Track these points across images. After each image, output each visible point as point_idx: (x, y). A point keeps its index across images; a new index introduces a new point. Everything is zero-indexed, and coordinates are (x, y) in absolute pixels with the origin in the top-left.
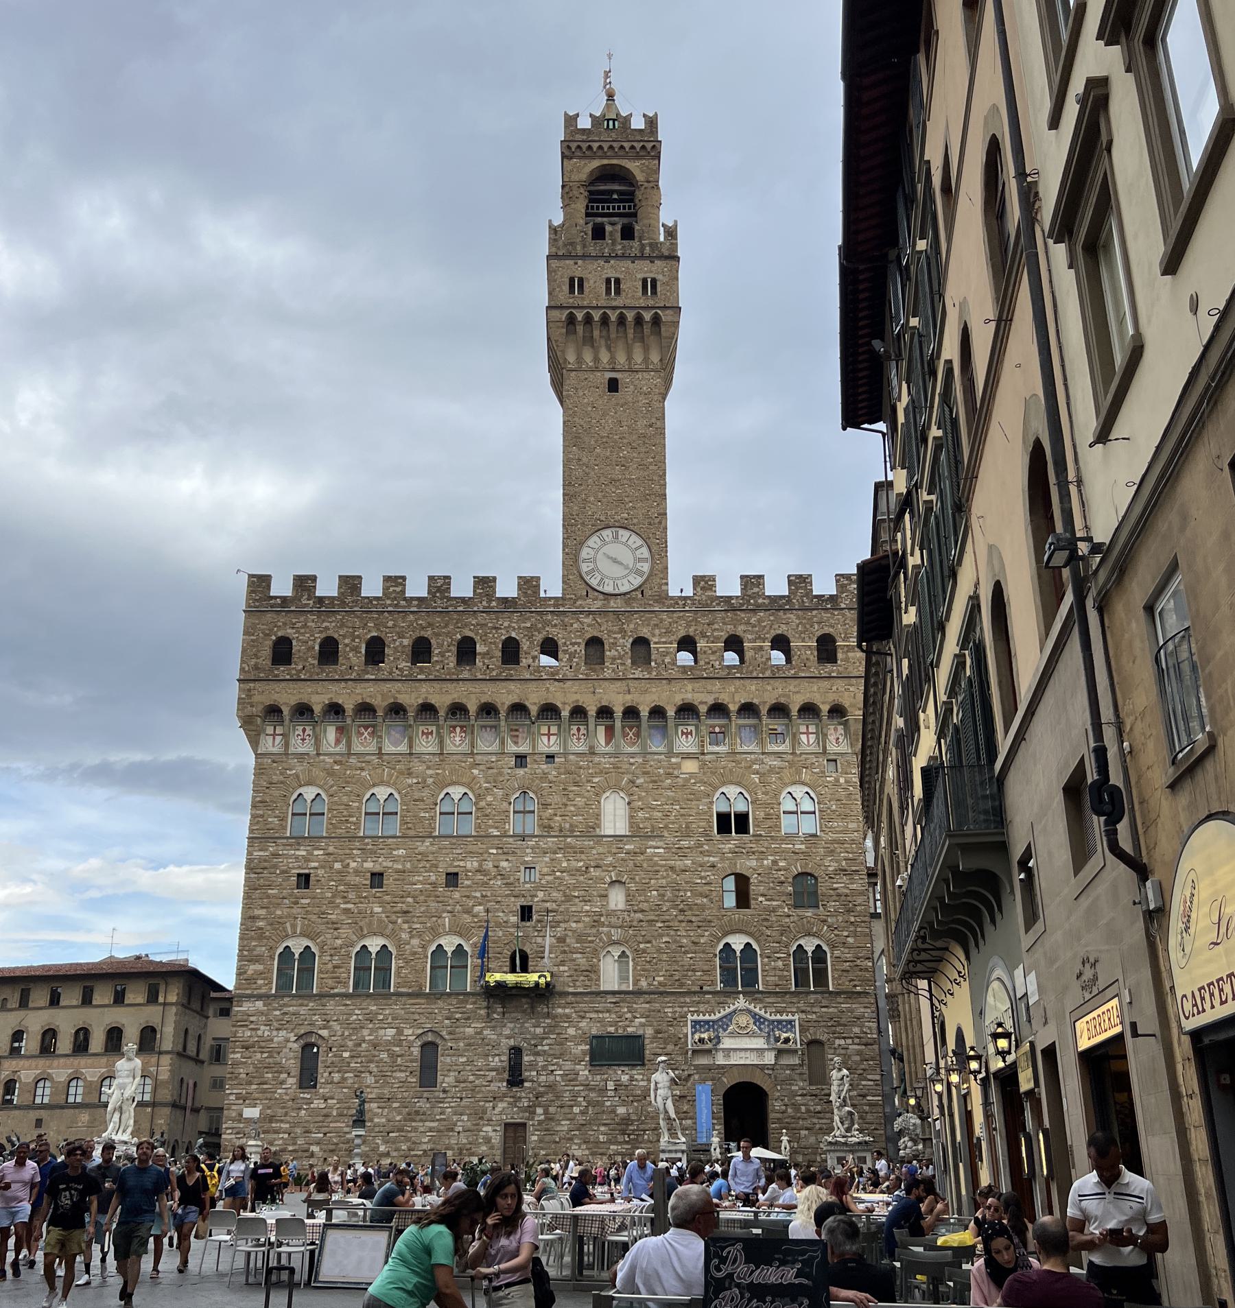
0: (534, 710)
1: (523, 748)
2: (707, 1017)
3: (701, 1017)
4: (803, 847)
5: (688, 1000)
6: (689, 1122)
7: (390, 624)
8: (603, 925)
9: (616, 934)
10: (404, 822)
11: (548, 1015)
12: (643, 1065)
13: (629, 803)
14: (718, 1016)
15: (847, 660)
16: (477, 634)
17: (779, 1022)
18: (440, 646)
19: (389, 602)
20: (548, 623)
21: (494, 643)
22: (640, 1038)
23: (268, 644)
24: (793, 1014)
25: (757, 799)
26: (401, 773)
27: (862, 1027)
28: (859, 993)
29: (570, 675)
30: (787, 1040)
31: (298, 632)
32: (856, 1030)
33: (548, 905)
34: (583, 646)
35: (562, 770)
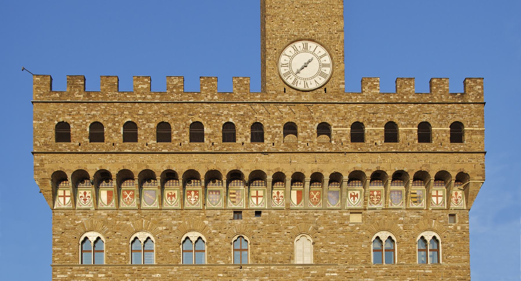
0: (247, 175)
1: (240, 205)
4: (431, 271)
7: (141, 112)
10: (158, 256)
13: (313, 243)
15: (471, 140)
16: (204, 120)
18: (178, 128)
19: (138, 96)
20: (255, 111)
21: (217, 126)
23: (52, 127)
25: (401, 241)
26: (155, 223)
29: (272, 150)
31: (73, 118)
34: (282, 129)
35: (267, 221)
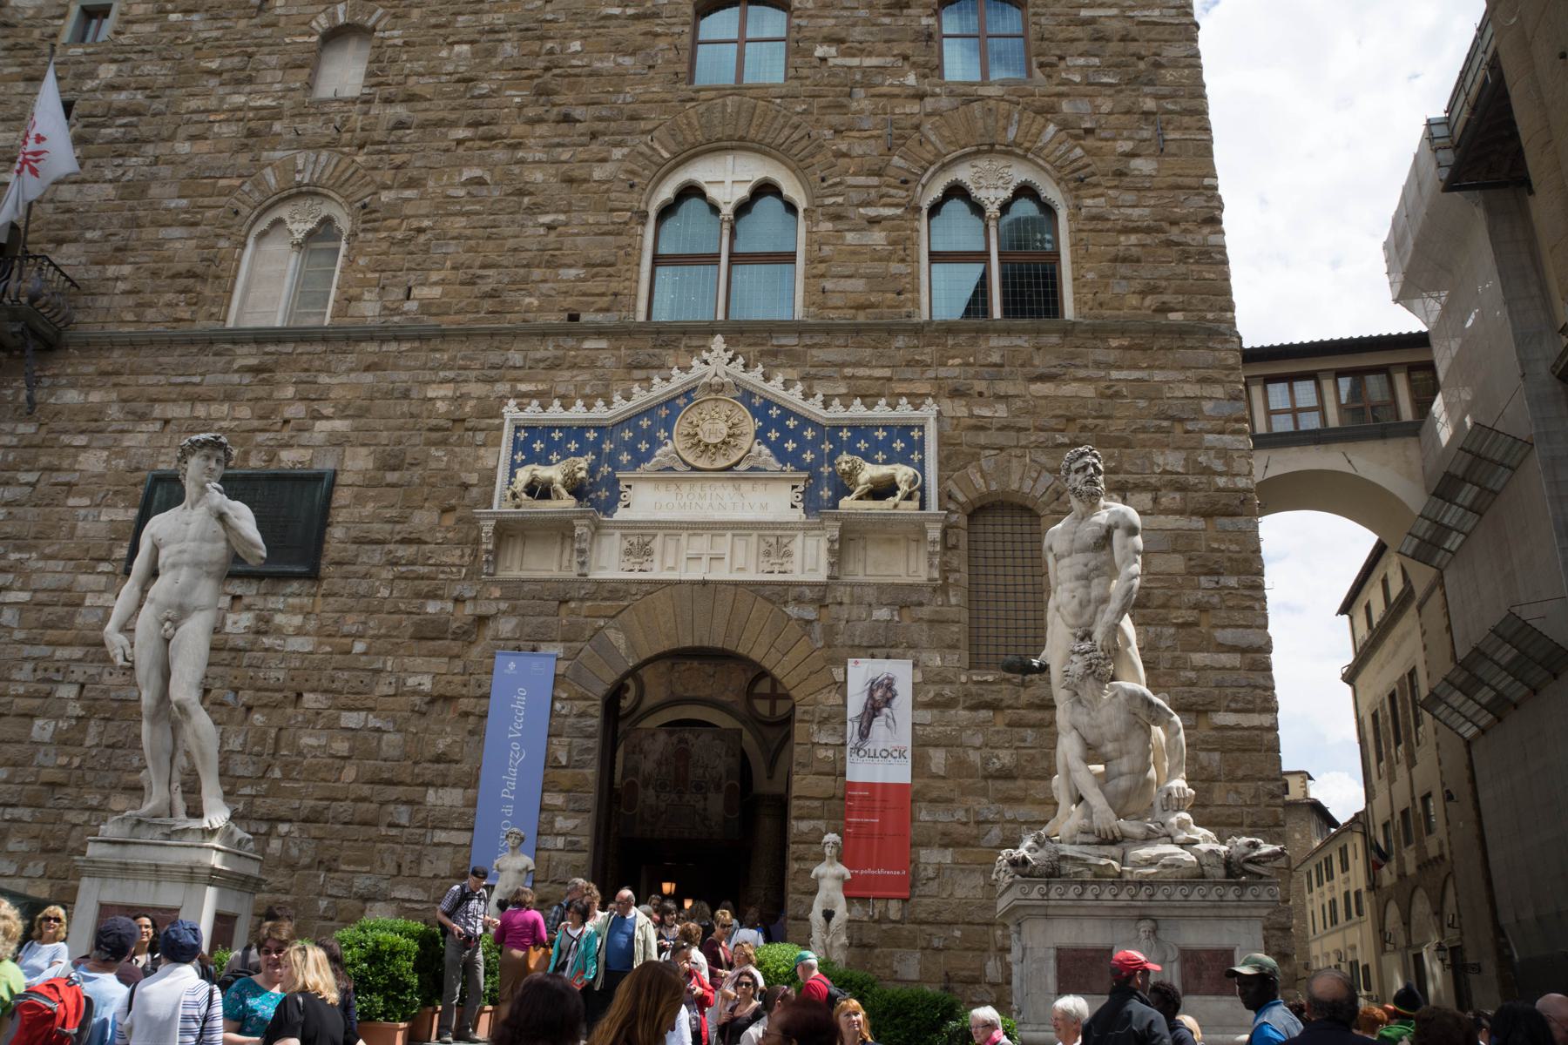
2: (578, 413)
3: (556, 412)
5: (515, 357)
6: (451, 798)
8: (275, 141)
9: (307, 165)
11: (31, 410)
12: (313, 576)
14: (621, 407)
17: (860, 430)
22: (318, 477)
24: (916, 400)
27: (1191, 446)
28: (1181, 332)
30: (883, 489)
32: (1172, 460)
33: (123, 96)
